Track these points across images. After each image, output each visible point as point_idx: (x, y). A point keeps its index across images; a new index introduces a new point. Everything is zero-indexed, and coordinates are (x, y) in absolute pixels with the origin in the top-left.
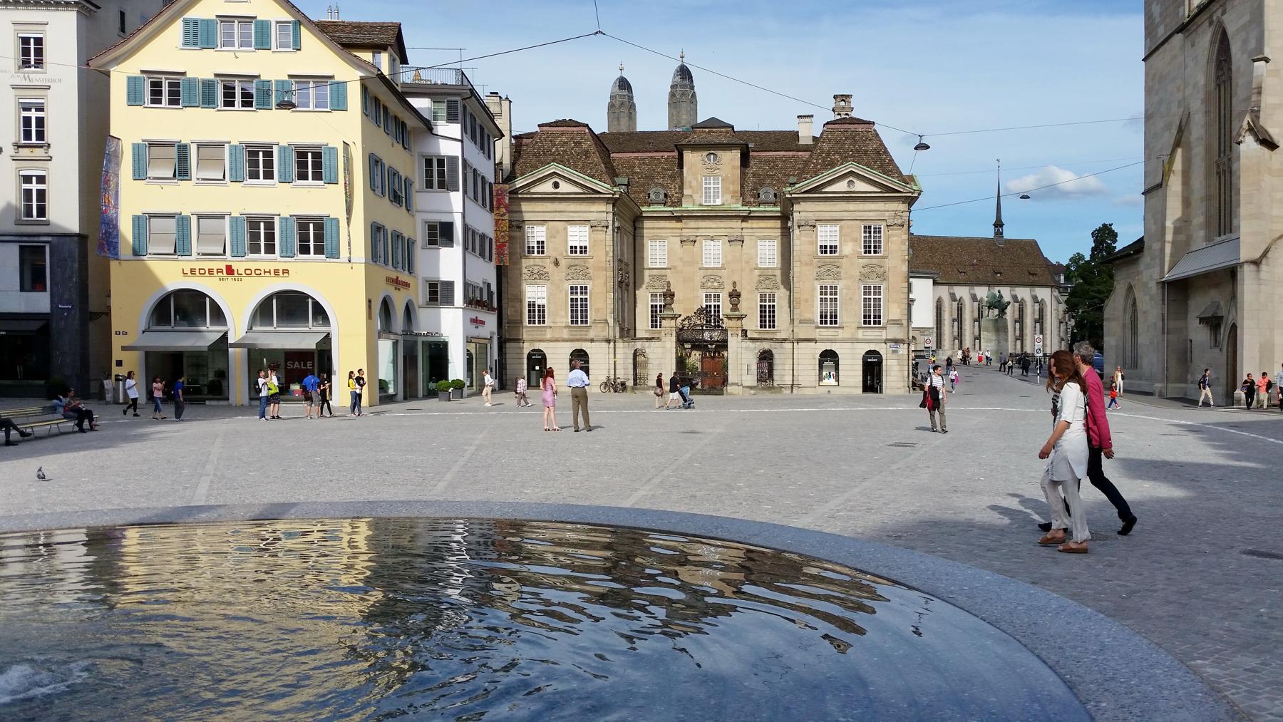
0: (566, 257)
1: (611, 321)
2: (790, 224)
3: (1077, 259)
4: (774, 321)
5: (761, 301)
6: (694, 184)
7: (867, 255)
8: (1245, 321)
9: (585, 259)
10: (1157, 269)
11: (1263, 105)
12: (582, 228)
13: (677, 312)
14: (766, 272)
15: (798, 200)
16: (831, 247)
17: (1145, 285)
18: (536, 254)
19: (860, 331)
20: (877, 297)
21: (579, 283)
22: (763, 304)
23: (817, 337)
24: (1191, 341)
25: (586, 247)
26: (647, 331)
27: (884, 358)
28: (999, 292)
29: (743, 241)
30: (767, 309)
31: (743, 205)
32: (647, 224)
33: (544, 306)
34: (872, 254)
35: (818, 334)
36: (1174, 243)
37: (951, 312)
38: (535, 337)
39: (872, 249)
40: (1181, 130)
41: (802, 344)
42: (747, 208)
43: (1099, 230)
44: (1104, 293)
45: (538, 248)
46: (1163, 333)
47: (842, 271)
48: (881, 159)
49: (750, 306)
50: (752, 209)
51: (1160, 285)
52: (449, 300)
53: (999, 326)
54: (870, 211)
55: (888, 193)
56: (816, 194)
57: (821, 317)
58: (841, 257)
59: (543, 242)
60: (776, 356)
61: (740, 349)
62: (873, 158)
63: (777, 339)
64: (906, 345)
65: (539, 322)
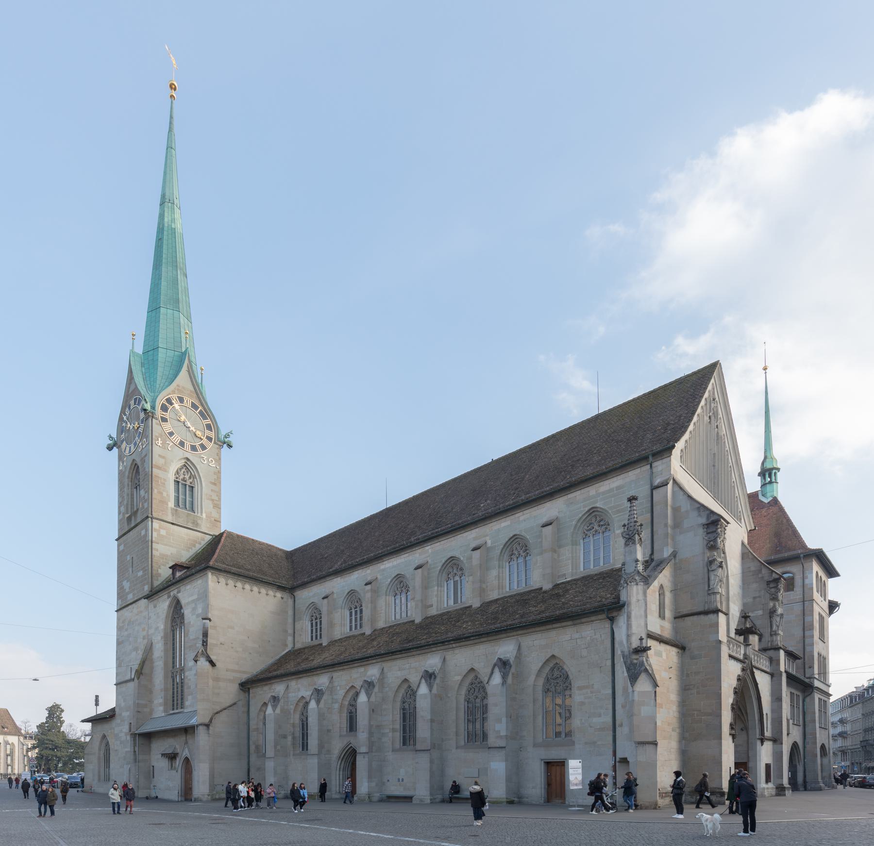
24: (153, 766)
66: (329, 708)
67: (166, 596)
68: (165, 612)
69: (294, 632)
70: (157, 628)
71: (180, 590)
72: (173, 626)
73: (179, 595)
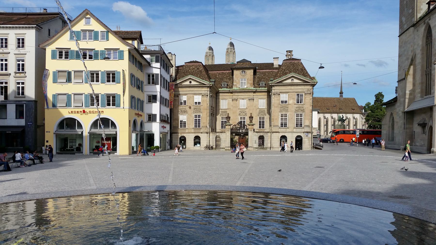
0: (193, 106)
1: (208, 127)
2: (271, 94)
3: (368, 104)
4: (264, 126)
5: (260, 119)
6: (237, 81)
7: (298, 104)
9: (200, 107)
10: (402, 107)
12: (199, 96)
13: (231, 123)
14: (261, 110)
15: (274, 86)
16: (285, 101)
17: (398, 113)
18: (183, 105)
20: (301, 118)
21: (198, 114)
22: (260, 120)
24: (414, 132)
25: (200, 102)
26: (220, 130)
28: (343, 115)
29: (254, 100)
30: (262, 122)
31: (254, 88)
32: (221, 94)
33: (185, 122)
34: (300, 103)
38: (182, 132)
39: (300, 102)
42: (255, 89)
45: (184, 103)
46: (404, 129)
47: (289, 109)
48: (303, 71)
49: (256, 121)
52: (155, 120)
54: (299, 89)
55: (305, 83)
56: (280, 84)
58: (289, 104)
59: (186, 101)
62: (300, 72)
65: (184, 127)
67: (423, 24)
68: (423, 33)
71: (430, 18)
72: (427, 42)
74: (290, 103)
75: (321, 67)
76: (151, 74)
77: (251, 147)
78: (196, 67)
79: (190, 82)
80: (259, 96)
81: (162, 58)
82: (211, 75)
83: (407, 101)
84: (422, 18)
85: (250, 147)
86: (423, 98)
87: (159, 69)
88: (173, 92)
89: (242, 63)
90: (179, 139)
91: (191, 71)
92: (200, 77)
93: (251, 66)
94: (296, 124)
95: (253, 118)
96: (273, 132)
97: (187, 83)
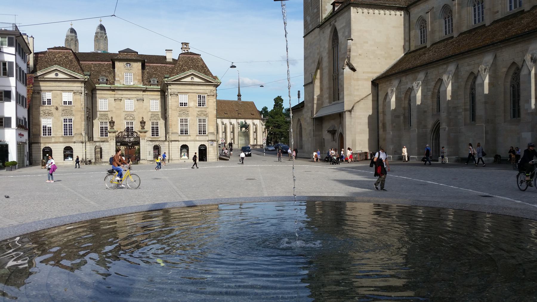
0: (62, 106)
1: (84, 134)
2: (166, 94)
4: (158, 133)
5: (152, 125)
6: (120, 75)
8: (347, 132)
9: (71, 107)
10: (310, 113)
11: (351, 56)
12: (69, 94)
13: (115, 130)
15: (170, 84)
16: (185, 103)
18: (47, 105)
19: (198, 137)
20: (204, 123)
21: (68, 118)
22: (153, 126)
23: (180, 140)
25: (71, 102)
26: (98, 138)
27: (207, 147)
30: (155, 128)
31: (143, 85)
32: (98, 92)
33: (50, 128)
35: (179, 138)
36: (317, 104)
37: (222, 129)
38: (46, 141)
39: (202, 105)
40: (319, 63)
41: (173, 143)
42: (145, 87)
43: (277, 98)
44: (279, 122)
45: (48, 102)
46: (314, 136)
47: (190, 113)
48: (203, 69)
49: (148, 127)
50: (147, 87)
51: (312, 119)
52: (9, 125)
53: (246, 135)
54: (200, 90)
55: (208, 83)
56: (178, 82)
57: (181, 131)
58: (190, 107)
59: (50, 100)
60: (162, 148)
61: (145, 145)
63: (162, 141)
64: (216, 142)
65: (48, 135)
66: (425, 95)
67: (329, 25)
68: (329, 36)
69: (410, 39)
70: (324, 47)
72: (333, 45)
73: (336, 23)
74: (190, 106)
75: (233, 67)
76: (2, 61)
77: (144, 160)
78: (64, 55)
79: (57, 75)
80: (150, 96)
81: (18, 41)
82: (84, 67)
83: (315, 106)
84: (328, 19)
85: (142, 160)
86: (331, 104)
87: (14, 56)
88: (32, 87)
89: (126, 53)
90: (42, 152)
91: (57, 59)
92: (69, 68)
93: (139, 58)
94: (199, 131)
95: (145, 123)
96: (171, 141)
97: (52, 75)
